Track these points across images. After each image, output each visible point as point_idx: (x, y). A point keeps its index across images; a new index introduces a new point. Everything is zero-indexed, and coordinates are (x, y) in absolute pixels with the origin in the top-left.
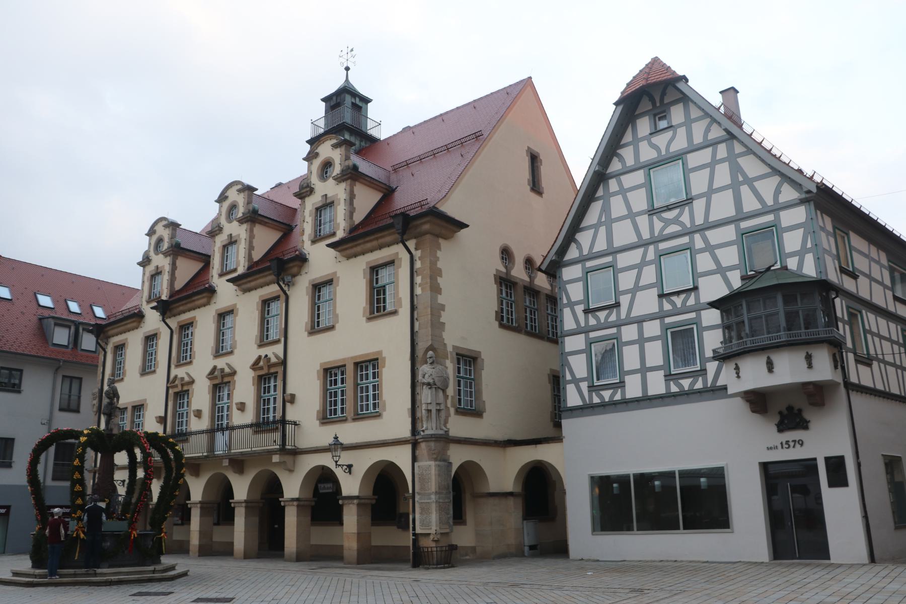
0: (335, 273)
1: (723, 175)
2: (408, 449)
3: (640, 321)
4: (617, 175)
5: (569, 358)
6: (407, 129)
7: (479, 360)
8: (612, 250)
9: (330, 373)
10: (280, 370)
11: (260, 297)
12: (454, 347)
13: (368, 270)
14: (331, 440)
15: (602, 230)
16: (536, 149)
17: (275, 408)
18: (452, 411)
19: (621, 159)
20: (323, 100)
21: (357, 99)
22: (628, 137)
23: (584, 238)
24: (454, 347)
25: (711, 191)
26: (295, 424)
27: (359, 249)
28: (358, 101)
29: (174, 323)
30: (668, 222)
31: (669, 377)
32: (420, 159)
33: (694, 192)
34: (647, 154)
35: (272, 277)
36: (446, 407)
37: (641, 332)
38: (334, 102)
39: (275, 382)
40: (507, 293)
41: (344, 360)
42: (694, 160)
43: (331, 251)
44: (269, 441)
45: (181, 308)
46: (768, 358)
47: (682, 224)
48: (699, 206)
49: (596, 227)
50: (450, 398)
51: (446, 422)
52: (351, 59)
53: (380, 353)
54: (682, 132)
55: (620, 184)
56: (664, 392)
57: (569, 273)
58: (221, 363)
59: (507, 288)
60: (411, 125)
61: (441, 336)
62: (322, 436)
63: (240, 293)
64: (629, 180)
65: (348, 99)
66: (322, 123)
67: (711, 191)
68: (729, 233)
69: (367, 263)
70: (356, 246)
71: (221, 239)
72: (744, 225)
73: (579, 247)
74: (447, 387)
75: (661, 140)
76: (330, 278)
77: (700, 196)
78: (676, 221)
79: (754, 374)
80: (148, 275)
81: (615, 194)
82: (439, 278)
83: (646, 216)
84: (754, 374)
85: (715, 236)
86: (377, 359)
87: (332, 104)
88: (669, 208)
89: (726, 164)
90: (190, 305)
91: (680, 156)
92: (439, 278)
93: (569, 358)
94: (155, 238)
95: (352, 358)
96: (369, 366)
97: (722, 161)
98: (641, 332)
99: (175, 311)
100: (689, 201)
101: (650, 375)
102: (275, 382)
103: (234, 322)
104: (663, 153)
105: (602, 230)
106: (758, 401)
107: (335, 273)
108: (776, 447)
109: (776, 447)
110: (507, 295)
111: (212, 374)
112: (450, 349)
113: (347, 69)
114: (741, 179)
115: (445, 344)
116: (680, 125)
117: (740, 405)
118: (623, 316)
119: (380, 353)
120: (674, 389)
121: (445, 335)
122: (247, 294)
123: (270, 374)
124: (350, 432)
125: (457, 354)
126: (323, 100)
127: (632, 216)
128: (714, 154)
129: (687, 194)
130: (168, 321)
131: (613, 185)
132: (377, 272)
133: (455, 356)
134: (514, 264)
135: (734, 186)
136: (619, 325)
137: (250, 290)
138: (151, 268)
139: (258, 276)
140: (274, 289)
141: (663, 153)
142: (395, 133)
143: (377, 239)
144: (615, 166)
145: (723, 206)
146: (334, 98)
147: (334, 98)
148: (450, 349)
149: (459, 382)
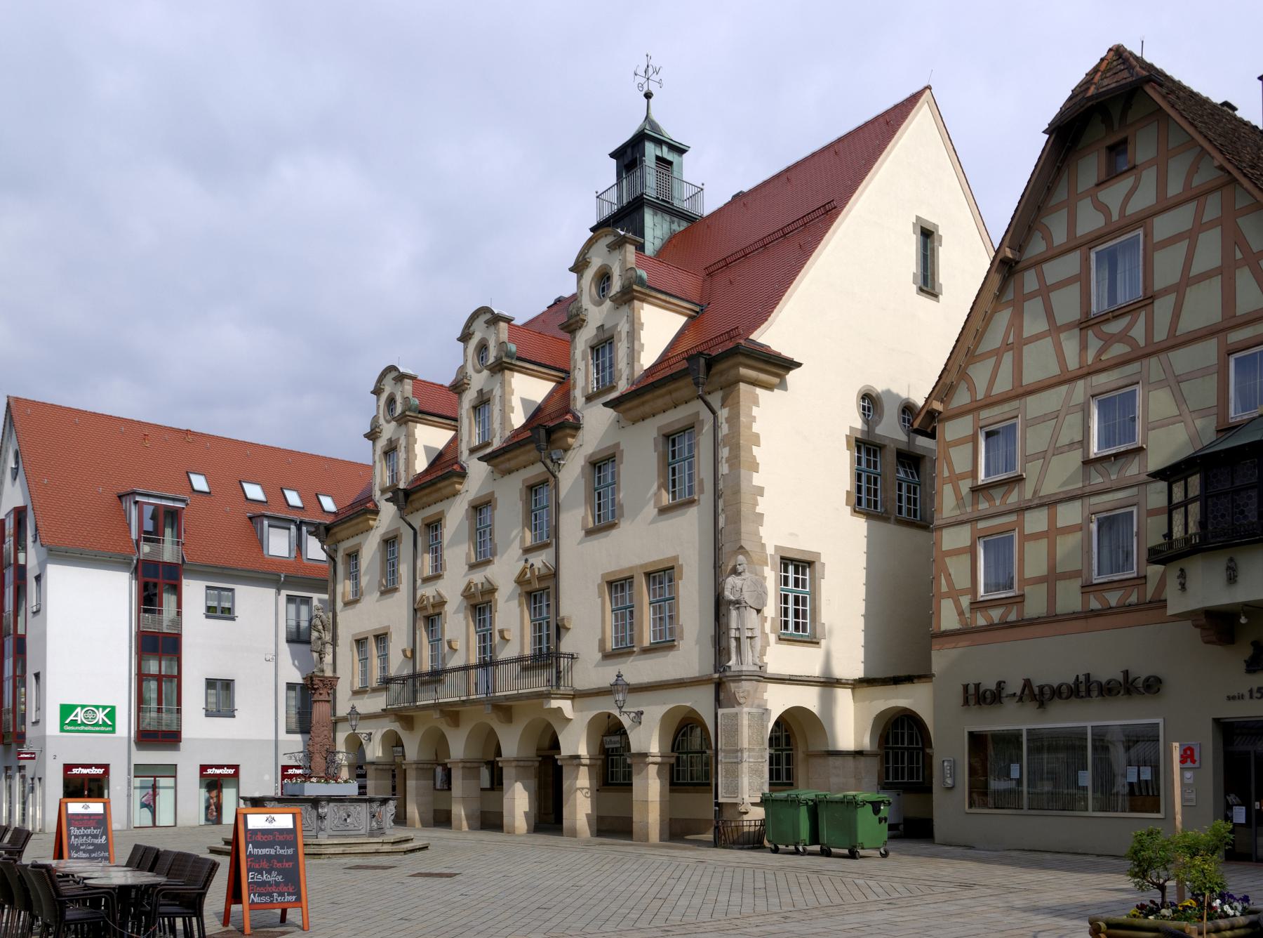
0: (618, 445)
1: (1209, 252)
2: (709, 691)
3: (1051, 503)
4: (1038, 263)
5: (947, 560)
6: (739, 197)
7: (817, 564)
8: (1020, 391)
9: (618, 585)
10: (551, 583)
11: (524, 481)
12: (777, 548)
13: (661, 439)
14: (613, 680)
15: (1008, 359)
16: (931, 217)
17: (548, 635)
18: (772, 638)
19: (1048, 237)
20: (612, 155)
21: (665, 149)
22: (1061, 194)
23: (980, 374)
24: (777, 548)
25: (1187, 281)
26: (572, 657)
27: (647, 408)
28: (666, 153)
29: (417, 520)
30: (1109, 340)
31: (1088, 588)
32: (745, 255)
33: (1158, 285)
34: (1089, 221)
35: (534, 454)
36: (763, 632)
37: (1052, 519)
38: (628, 157)
39: (548, 600)
40: (868, 461)
41: (631, 568)
42: (1164, 226)
43: (610, 412)
44: (538, 682)
45: (425, 500)
46: (1231, 560)
47: (1132, 342)
48: (1163, 308)
49: (997, 353)
50: (769, 620)
51: (763, 653)
52: (654, 77)
53: (676, 558)
54: (1149, 178)
55: (1041, 277)
56: (1079, 608)
57: (953, 430)
58: (478, 577)
59: (868, 454)
60: (745, 190)
61: (757, 534)
62: (604, 676)
63: (497, 476)
64: (1057, 270)
65: (651, 150)
66: (613, 196)
67: (1187, 281)
68: (1208, 352)
69: (659, 429)
70: (643, 404)
71: (469, 397)
72: (1236, 337)
73: (972, 388)
74: (764, 604)
75: (1113, 195)
76: (611, 452)
77: (1165, 291)
78: (1123, 337)
79: (1207, 587)
80: (379, 452)
81: (1032, 295)
82: (754, 448)
83: (1077, 331)
84: (1207, 587)
85: (1182, 360)
86: (672, 568)
87: (626, 162)
88: (1116, 315)
89: (1217, 231)
90: (435, 496)
91: (1144, 220)
92: (754, 448)
93: (947, 560)
94: (384, 396)
95: (642, 566)
96: (662, 576)
97: (1211, 225)
98: (1052, 519)
99: (416, 505)
100: (1148, 300)
101: (1060, 585)
102: (548, 600)
103: (492, 519)
104: (1115, 217)
105: (1008, 359)
106: (1220, 625)
107: (618, 445)
108: (1241, 697)
109: (1241, 697)
110: (868, 466)
111: (468, 594)
112: (770, 550)
113: (648, 96)
114: (1239, 255)
115: (763, 545)
116: (1148, 164)
117: (1190, 632)
118: (1028, 494)
119: (676, 558)
120: (1095, 604)
121: (763, 531)
122: (507, 478)
123: (540, 592)
124: (638, 670)
125: (782, 558)
126: (612, 155)
127: (1055, 329)
128: (1199, 213)
129: (1145, 289)
130: (408, 518)
131: (1030, 281)
132: (674, 441)
133: (779, 561)
134: (881, 416)
135: (1226, 272)
136: (1021, 510)
137: (510, 472)
138: (382, 443)
139: (518, 452)
140: (536, 470)
141: (1115, 217)
142: (721, 204)
143: (670, 393)
144: (1037, 247)
145: (1203, 307)
146: (629, 151)
147: (629, 151)
148: (770, 550)
149: (786, 597)
